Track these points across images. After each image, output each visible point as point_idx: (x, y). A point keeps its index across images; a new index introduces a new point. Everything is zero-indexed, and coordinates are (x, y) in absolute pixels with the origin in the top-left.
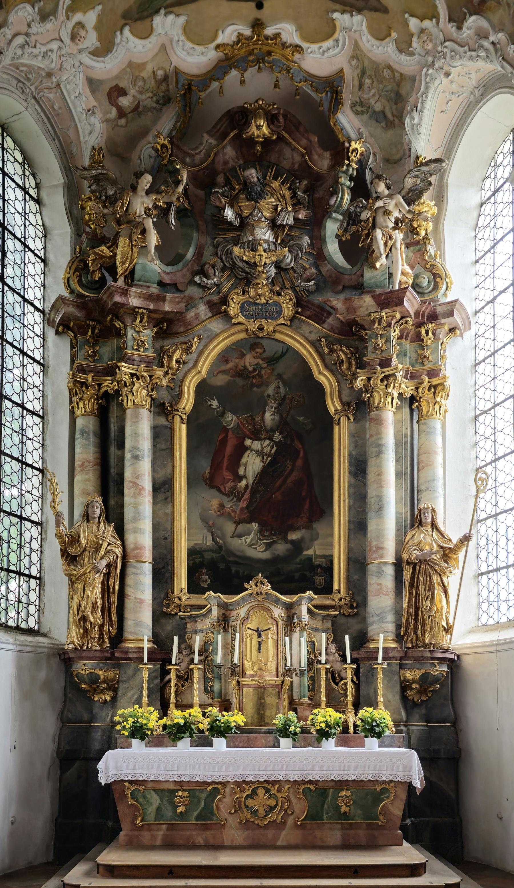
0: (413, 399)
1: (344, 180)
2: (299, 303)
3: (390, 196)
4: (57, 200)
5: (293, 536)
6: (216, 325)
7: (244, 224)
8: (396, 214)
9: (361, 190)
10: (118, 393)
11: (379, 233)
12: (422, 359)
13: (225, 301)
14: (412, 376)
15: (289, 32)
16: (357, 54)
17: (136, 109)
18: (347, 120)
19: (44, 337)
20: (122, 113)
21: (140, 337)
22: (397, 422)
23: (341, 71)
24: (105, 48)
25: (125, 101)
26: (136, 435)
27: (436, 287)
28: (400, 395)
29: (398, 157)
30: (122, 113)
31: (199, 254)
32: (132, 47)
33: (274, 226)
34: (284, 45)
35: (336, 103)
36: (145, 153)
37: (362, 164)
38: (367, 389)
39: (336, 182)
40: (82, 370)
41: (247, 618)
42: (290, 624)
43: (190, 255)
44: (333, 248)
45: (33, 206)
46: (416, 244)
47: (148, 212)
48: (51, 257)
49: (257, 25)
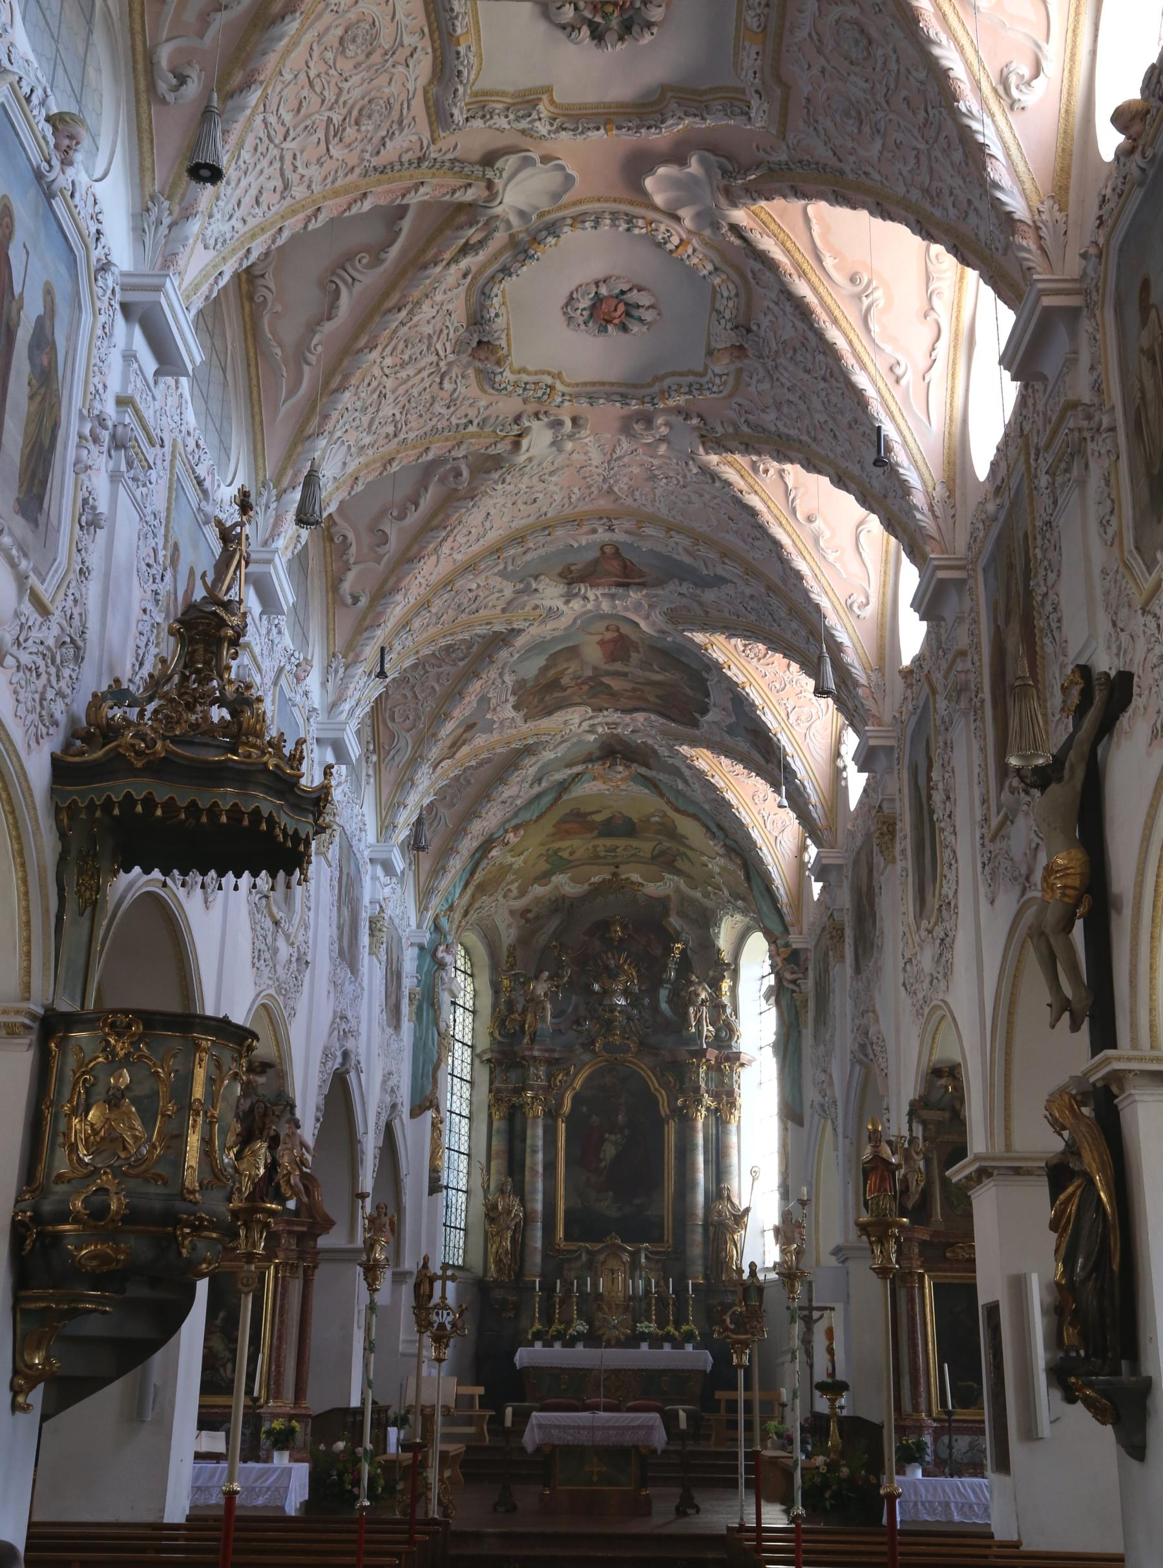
0: (717, 1110)
1: (672, 965)
2: (641, 1044)
3: (699, 983)
4: (484, 978)
5: (637, 1201)
6: (586, 1057)
7: (607, 992)
8: (703, 995)
9: (685, 965)
10: (522, 1106)
11: (691, 1010)
12: (721, 1083)
13: (593, 1043)
14: (716, 1096)
15: (636, 877)
16: (678, 890)
17: (537, 917)
18: (675, 921)
19: (472, 1064)
20: (528, 921)
21: (538, 1074)
22: (705, 1125)
23: (669, 896)
24: (523, 892)
25: (530, 915)
26: (534, 1137)
27: (731, 1038)
28: (708, 1109)
29: (708, 946)
30: (528, 921)
31: (576, 1009)
32: (538, 890)
33: (626, 993)
34: (632, 883)
35: (666, 912)
36: (542, 939)
37: (683, 952)
38: (685, 1106)
39: (666, 965)
40: (499, 1091)
41: (604, 1262)
42: (634, 1265)
43: (570, 1010)
44: (664, 1006)
45: (469, 980)
46: (717, 1007)
47: (546, 995)
48: (478, 1008)
49: (615, 875)
